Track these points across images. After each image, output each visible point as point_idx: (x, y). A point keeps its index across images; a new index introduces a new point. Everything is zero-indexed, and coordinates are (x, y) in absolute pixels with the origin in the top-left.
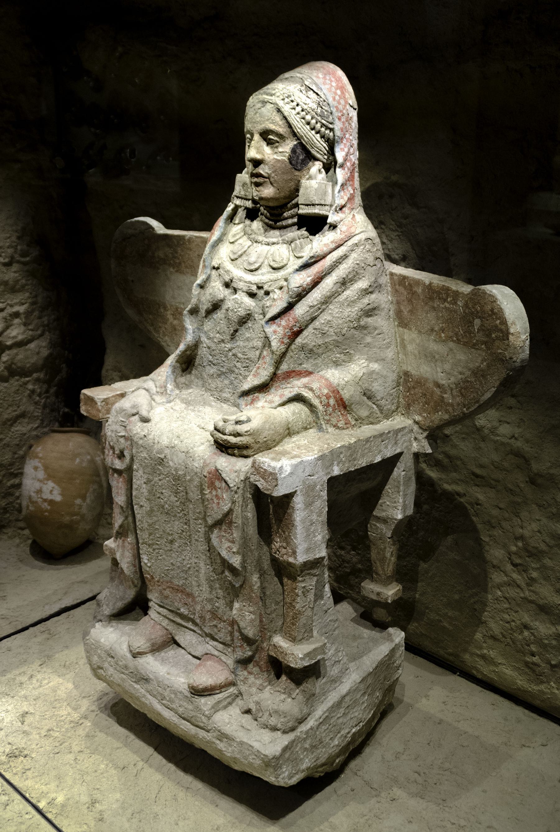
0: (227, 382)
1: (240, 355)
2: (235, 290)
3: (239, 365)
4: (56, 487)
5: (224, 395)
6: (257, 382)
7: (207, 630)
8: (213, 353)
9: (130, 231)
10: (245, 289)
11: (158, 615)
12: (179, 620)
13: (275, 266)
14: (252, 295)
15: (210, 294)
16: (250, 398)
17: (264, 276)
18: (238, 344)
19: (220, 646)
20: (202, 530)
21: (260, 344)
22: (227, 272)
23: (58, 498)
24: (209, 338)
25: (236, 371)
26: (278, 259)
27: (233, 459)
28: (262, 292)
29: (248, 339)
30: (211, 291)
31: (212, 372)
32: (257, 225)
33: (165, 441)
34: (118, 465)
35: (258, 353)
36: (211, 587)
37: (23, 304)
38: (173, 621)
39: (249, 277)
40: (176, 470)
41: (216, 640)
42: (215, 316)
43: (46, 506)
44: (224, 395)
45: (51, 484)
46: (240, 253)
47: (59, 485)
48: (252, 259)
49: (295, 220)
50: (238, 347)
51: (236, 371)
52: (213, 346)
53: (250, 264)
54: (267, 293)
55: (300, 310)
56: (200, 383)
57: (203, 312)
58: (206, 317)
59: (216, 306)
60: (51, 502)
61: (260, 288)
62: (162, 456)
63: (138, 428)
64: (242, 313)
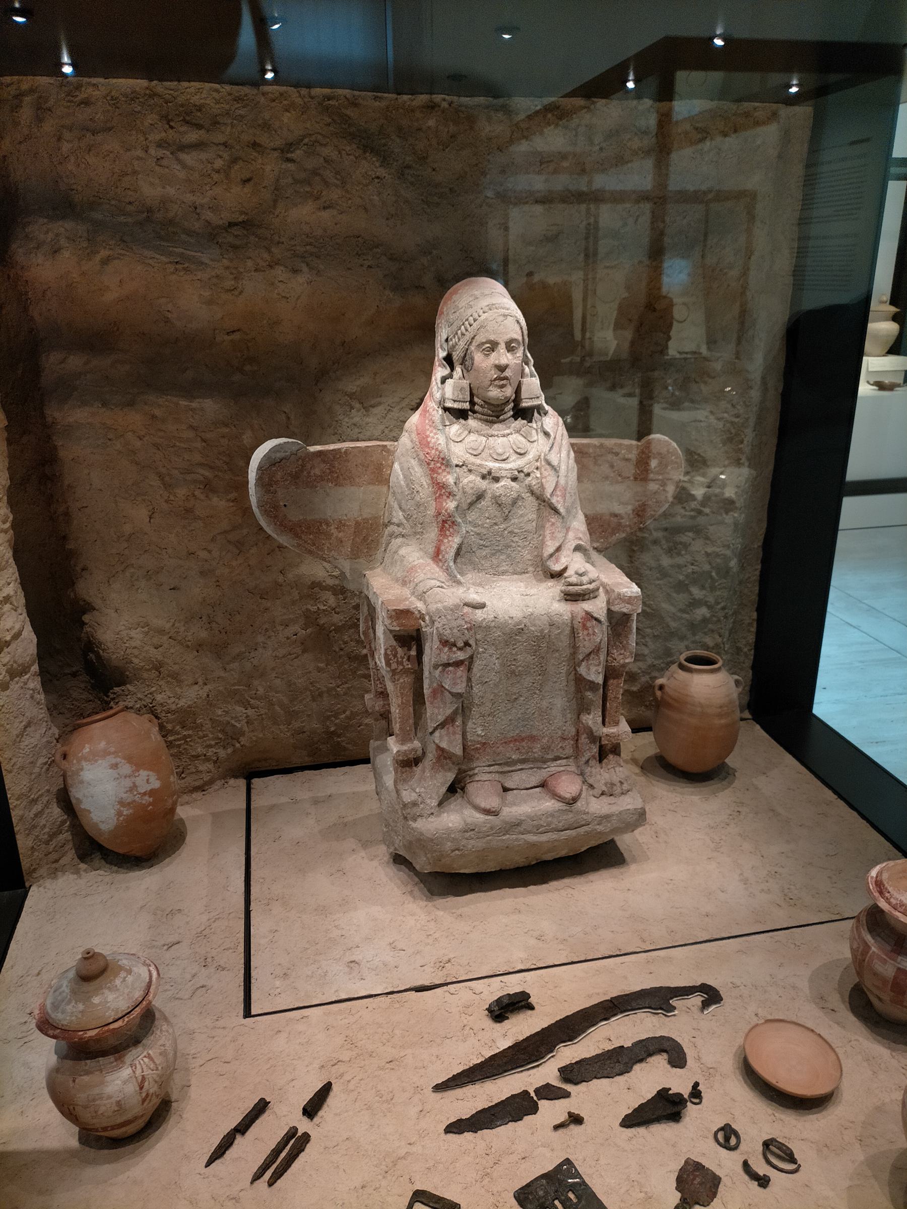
0: (503, 557)
1: (516, 531)
2: (497, 479)
3: (516, 539)
4: (151, 773)
5: (501, 569)
6: (557, 545)
7: (550, 756)
8: (484, 537)
9: (279, 455)
10: (509, 475)
11: (488, 775)
12: (507, 769)
13: (522, 452)
14: (514, 479)
15: (472, 488)
16: (554, 558)
17: (515, 463)
18: (513, 521)
19: (564, 762)
20: (564, 669)
21: (535, 516)
22: (480, 466)
23: (156, 784)
24: (476, 526)
25: (514, 545)
26: (520, 446)
27: (590, 602)
28: (522, 474)
29: (521, 516)
30: (471, 485)
31: (484, 553)
32: (472, 422)
33: (516, 613)
34: (461, 656)
35: (534, 524)
36: (564, 716)
37: (9, 584)
38: (501, 773)
39: (503, 465)
40: (542, 631)
41: (560, 758)
42: (479, 506)
43: (148, 799)
44: (501, 569)
45: (144, 773)
46: (481, 448)
47: (151, 770)
48: (500, 451)
49: (512, 413)
50: (514, 524)
51: (514, 545)
52: (484, 531)
53: (498, 454)
54: (528, 475)
55: (562, 481)
56: (470, 568)
57: (465, 506)
58: (468, 509)
59: (480, 496)
60: (152, 793)
61: (519, 472)
62: (523, 626)
63: (479, 615)
64: (514, 495)
